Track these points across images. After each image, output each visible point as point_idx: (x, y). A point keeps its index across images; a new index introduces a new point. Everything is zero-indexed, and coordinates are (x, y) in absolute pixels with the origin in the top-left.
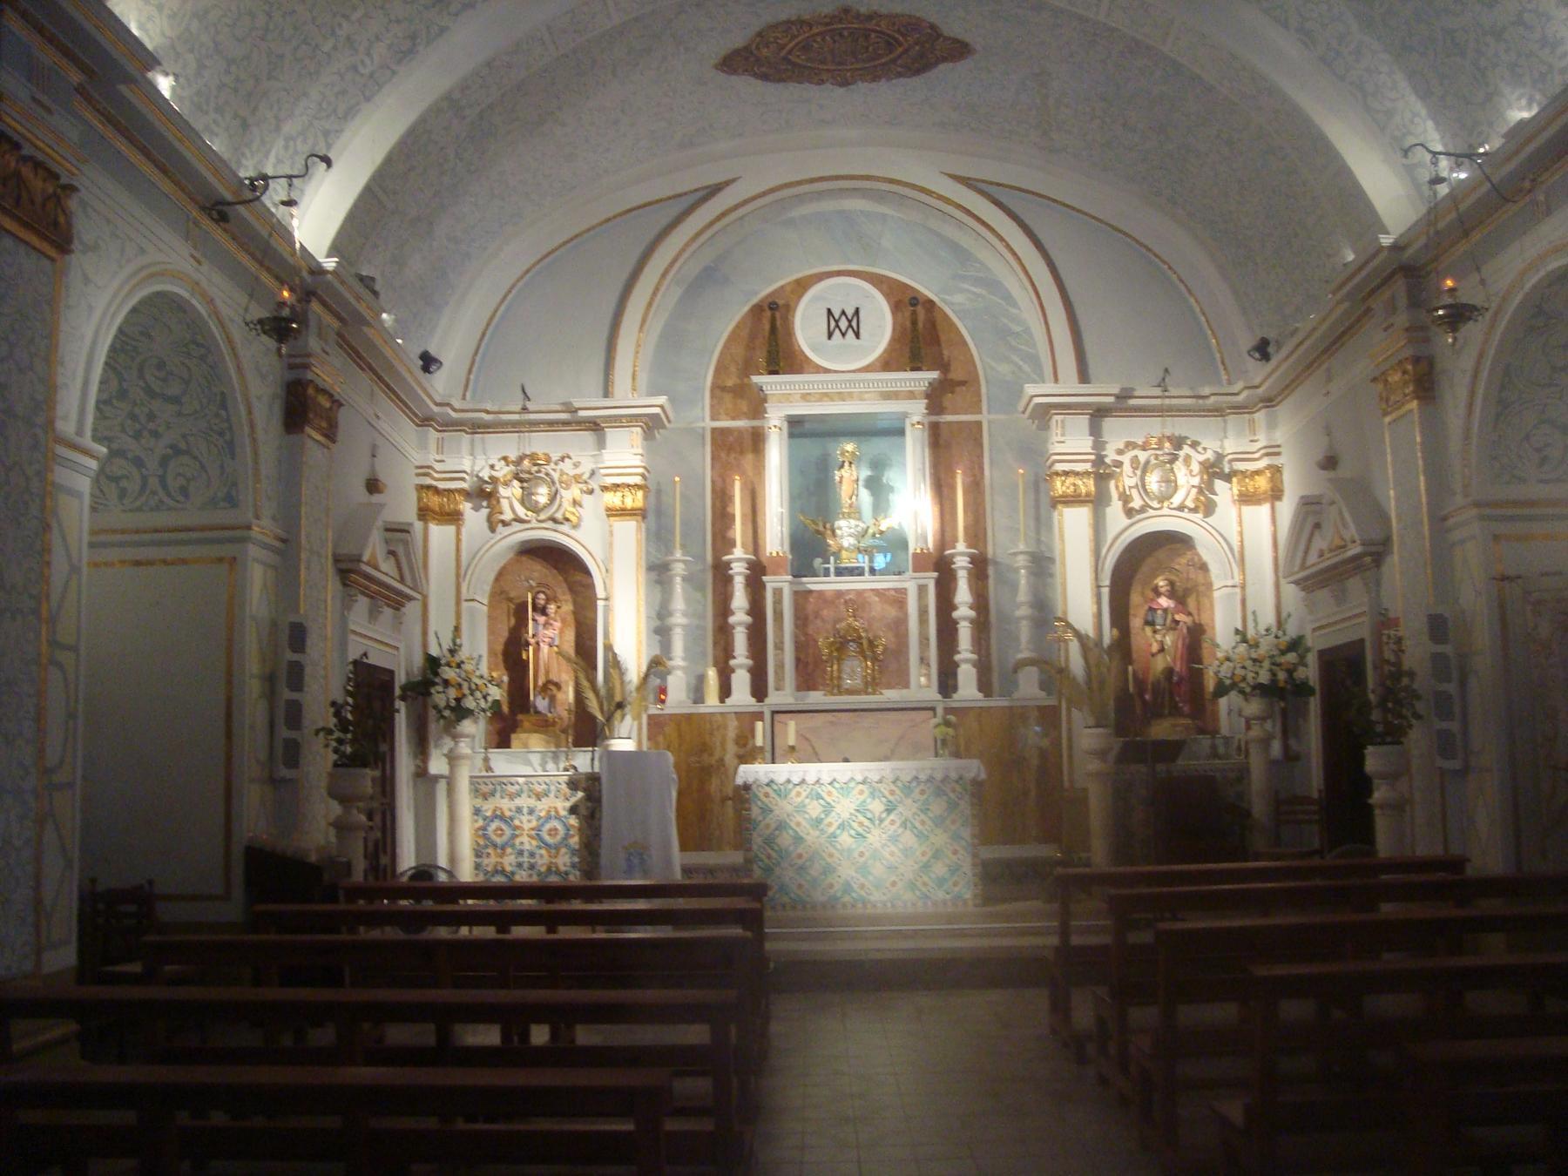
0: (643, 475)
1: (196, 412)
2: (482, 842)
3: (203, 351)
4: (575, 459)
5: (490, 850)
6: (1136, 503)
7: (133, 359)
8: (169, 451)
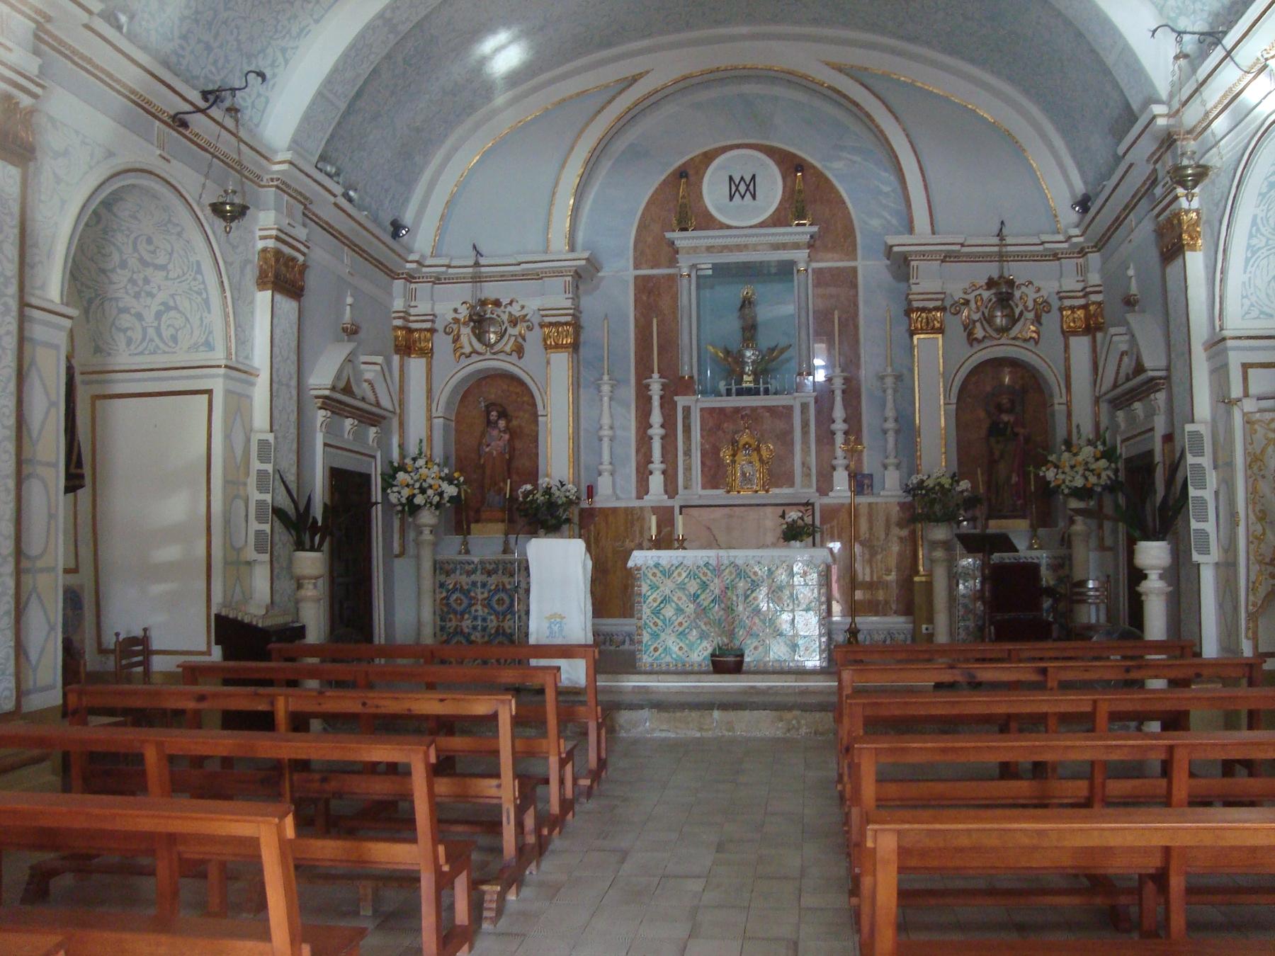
0: (573, 315)
1: (178, 277)
2: (445, 610)
3: (179, 229)
4: (521, 303)
5: (452, 616)
6: (979, 333)
7: (128, 236)
8: (162, 308)
